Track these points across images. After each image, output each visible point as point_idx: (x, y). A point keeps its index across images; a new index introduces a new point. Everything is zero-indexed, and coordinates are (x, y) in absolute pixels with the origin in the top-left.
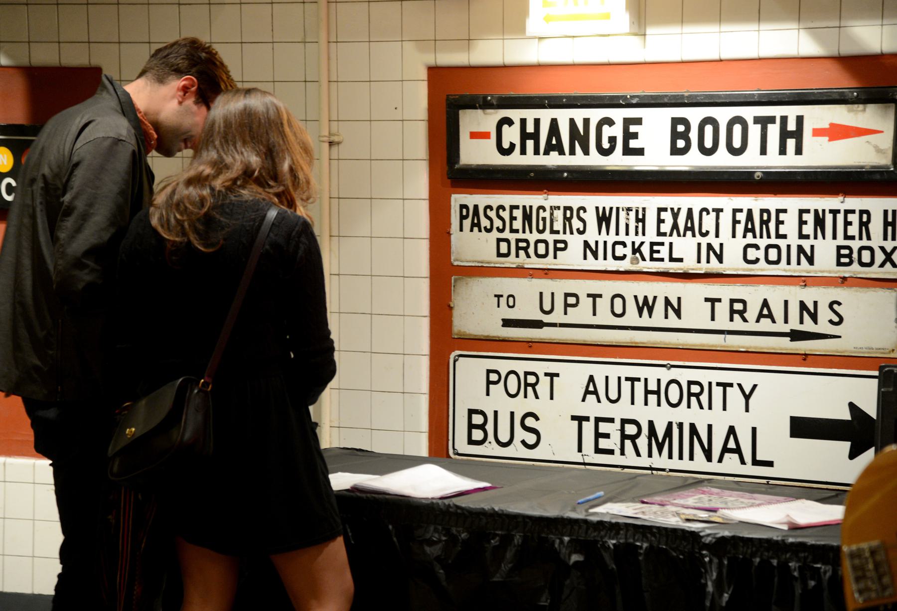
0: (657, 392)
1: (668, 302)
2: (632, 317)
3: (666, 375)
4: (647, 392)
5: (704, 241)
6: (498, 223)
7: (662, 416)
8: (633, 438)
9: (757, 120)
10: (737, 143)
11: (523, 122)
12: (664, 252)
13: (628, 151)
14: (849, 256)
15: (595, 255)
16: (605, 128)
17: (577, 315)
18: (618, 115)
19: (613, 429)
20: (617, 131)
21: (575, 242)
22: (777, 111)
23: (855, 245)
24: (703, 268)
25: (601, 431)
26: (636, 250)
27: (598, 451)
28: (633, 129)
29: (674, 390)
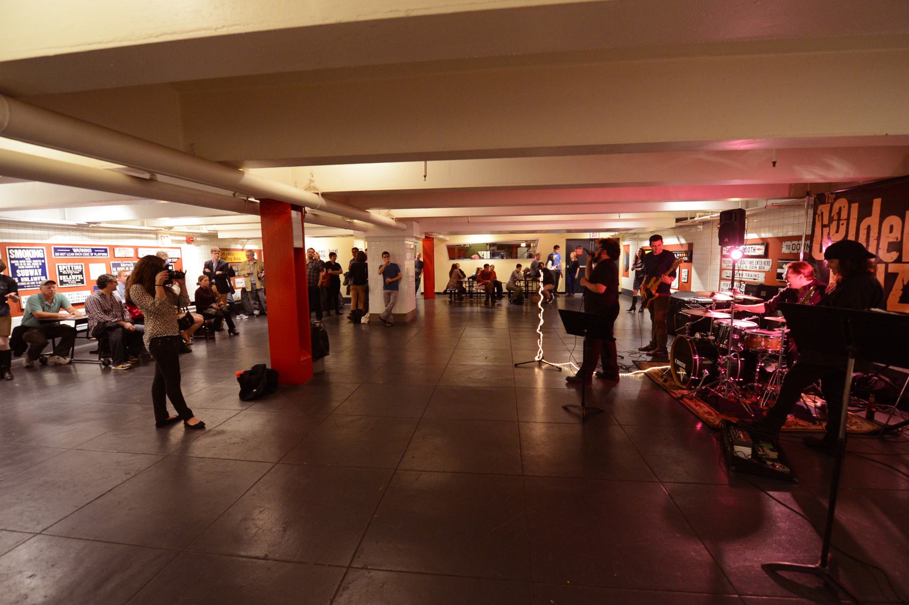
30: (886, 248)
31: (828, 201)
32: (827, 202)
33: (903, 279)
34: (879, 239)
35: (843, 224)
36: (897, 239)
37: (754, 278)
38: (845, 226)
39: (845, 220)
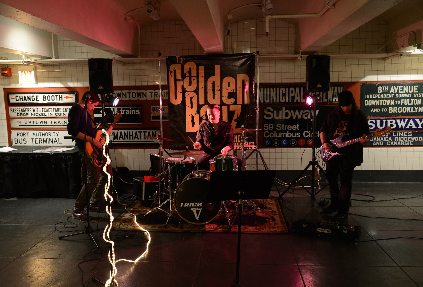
0: (44, 134)
1: (45, 122)
2: (39, 124)
4: (43, 134)
5: (49, 113)
6: (17, 111)
7: (45, 138)
8: (41, 141)
9: (56, 96)
10: (53, 99)
11: (20, 96)
13: (37, 100)
15: (33, 115)
16: (33, 97)
18: (35, 95)
19: (38, 140)
20: (35, 97)
24: (50, 116)
25: (36, 140)
26: (39, 114)
28: (37, 97)
29: (47, 134)
30: (227, 96)
31: (179, 62)
32: (178, 63)
33: (238, 114)
35: (194, 80)
36: (234, 91)
37: (63, 124)
38: (196, 80)
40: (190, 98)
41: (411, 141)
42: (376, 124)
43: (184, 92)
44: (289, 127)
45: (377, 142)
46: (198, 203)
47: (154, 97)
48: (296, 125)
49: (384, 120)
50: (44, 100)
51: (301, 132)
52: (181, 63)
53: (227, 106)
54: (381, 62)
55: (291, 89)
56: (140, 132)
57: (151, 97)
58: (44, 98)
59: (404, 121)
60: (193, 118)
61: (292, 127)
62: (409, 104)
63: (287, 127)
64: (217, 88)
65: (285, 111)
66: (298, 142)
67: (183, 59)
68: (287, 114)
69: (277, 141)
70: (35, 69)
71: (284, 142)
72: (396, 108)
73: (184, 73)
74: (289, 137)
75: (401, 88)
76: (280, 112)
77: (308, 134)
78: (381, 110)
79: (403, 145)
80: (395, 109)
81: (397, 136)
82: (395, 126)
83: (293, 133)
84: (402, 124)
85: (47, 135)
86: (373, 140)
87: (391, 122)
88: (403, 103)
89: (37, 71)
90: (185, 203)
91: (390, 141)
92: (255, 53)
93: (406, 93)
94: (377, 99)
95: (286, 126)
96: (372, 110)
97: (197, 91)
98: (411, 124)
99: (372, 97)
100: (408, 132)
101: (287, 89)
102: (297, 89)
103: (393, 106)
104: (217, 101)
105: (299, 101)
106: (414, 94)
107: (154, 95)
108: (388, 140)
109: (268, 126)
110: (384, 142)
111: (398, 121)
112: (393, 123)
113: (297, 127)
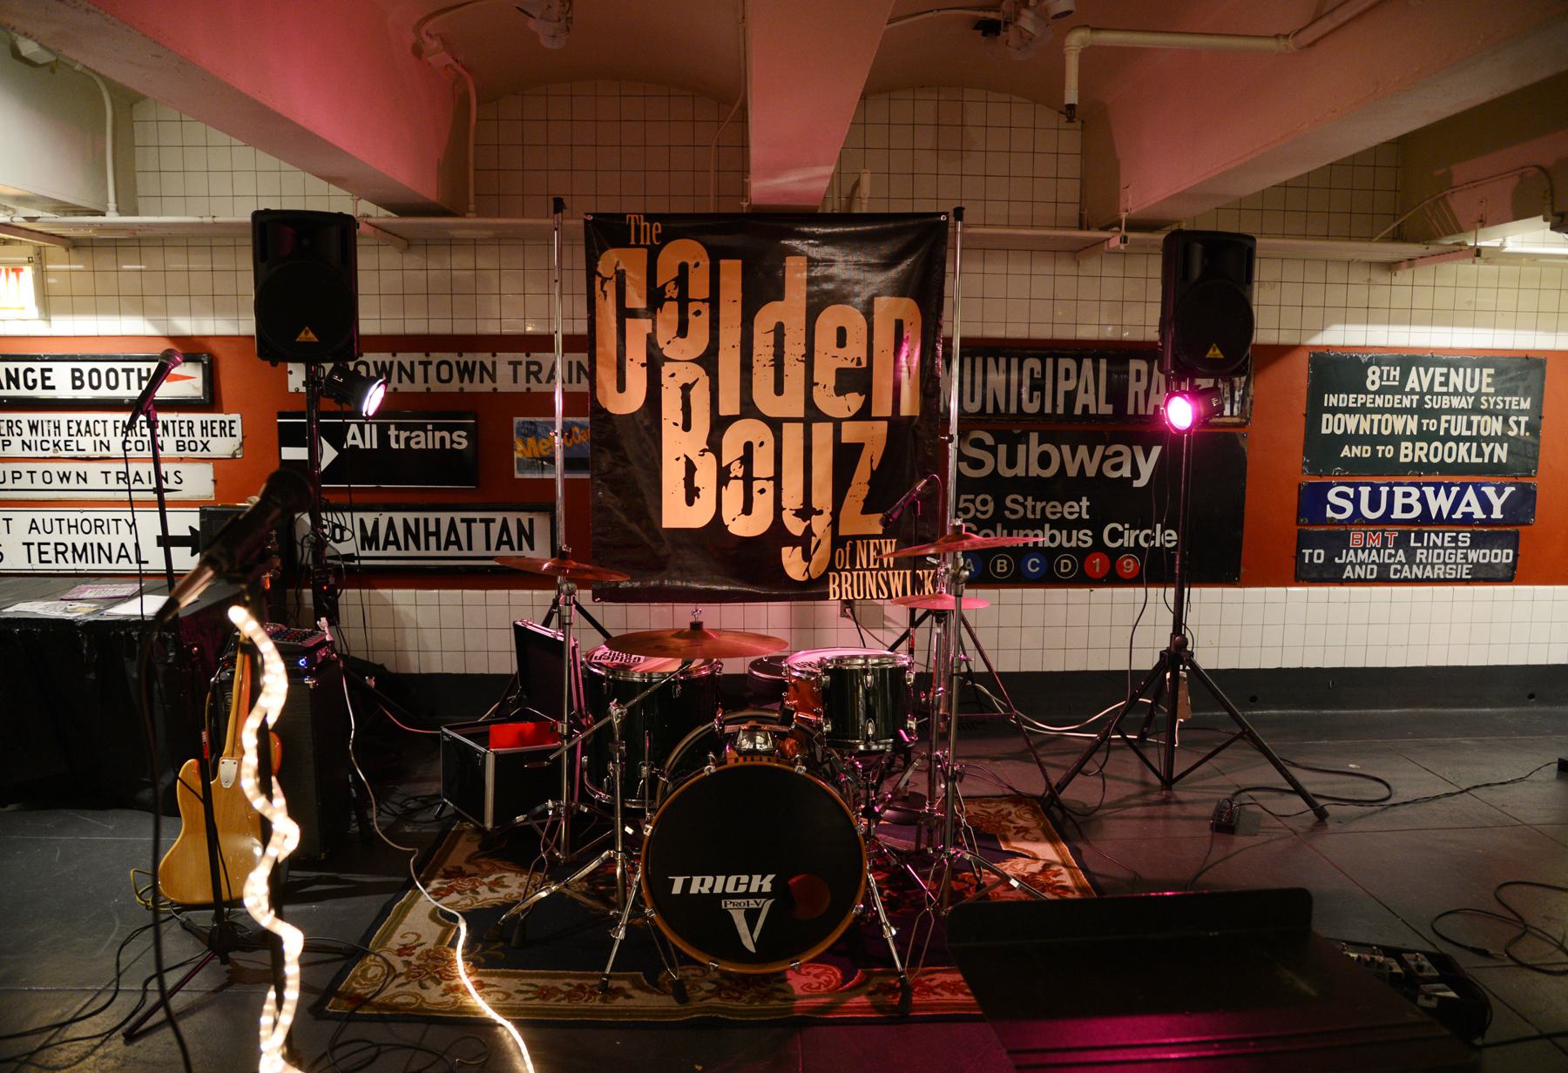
0: (76, 526)
1: (78, 475)
2: (56, 484)
3: (81, 517)
4: (70, 526)
5: (98, 439)
7: (80, 540)
8: (63, 553)
9: (124, 370)
10: (113, 383)
12: (73, 446)
13: (44, 387)
14: (184, 446)
15: (30, 448)
16: (29, 373)
17: (19, 484)
18: (37, 366)
19: (50, 549)
20: (37, 375)
21: (16, 441)
22: (135, 365)
23: (186, 440)
24: (98, 454)
25: (42, 550)
26: (56, 445)
27: (41, 561)
28: (47, 374)
29: (86, 524)
30: (832, 383)
31: (638, 239)
32: (633, 242)
34: (809, 359)
35: (698, 313)
36: (859, 362)
38: (706, 315)
39: (704, 301)
40: (681, 388)
41: (1467, 563)
42: (1356, 501)
43: (654, 364)
44: (1053, 509)
45: (1357, 567)
46: (756, 878)
47: (528, 381)
48: (1079, 501)
49: (1381, 489)
50: (75, 387)
51: (1095, 526)
52: (648, 243)
53: (830, 425)
54: (1381, 277)
55: (1066, 363)
56: (469, 522)
57: (515, 381)
58: (76, 379)
59: (1448, 495)
60: (690, 468)
61: (1063, 507)
62: (1466, 433)
63: (1043, 509)
64: (794, 348)
65: (1039, 445)
66: (1081, 565)
67: (657, 229)
68: (1044, 460)
69: (1005, 562)
70: (39, 261)
71: (1032, 565)
72: (1425, 445)
73: (659, 285)
74: (1053, 545)
75: (1441, 375)
76: (1021, 448)
77: (1121, 535)
78: (1374, 452)
79: (1442, 577)
80: (1421, 449)
81: (1422, 547)
82: (1417, 510)
83: (1065, 532)
84: (1440, 503)
85: (86, 524)
86: (1342, 561)
87: (1407, 495)
88: (1447, 430)
89: (48, 267)
90: (691, 879)
91: (1400, 562)
92: (946, 214)
93: (1456, 393)
94: (1364, 410)
95: (1039, 505)
96: (1346, 452)
97: (709, 361)
98: (1468, 504)
99: (1345, 405)
100: (1458, 533)
101: (1050, 361)
102: (1087, 363)
103: (1413, 439)
104: (791, 404)
105: (1092, 410)
106: (1483, 399)
107: (529, 373)
108: (1392, 560)
109: (973, 501)
110: (1379, 565)
111: (1429, 491)
112: (1413, 500)
113: (1080, 507)
